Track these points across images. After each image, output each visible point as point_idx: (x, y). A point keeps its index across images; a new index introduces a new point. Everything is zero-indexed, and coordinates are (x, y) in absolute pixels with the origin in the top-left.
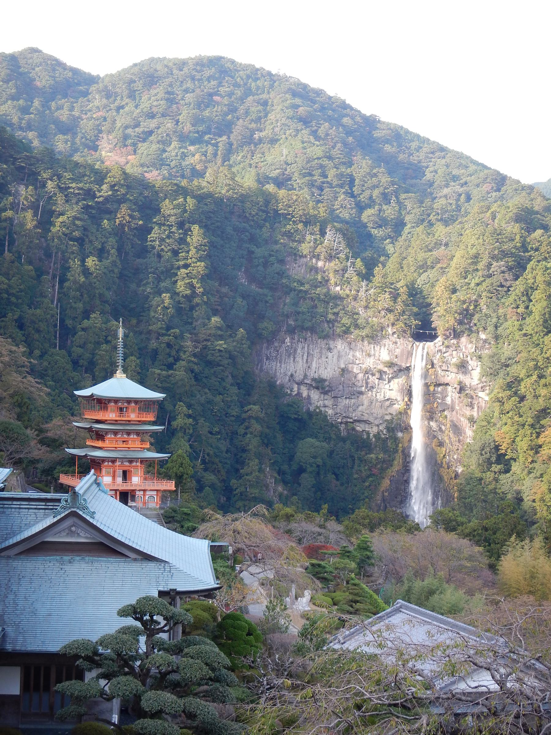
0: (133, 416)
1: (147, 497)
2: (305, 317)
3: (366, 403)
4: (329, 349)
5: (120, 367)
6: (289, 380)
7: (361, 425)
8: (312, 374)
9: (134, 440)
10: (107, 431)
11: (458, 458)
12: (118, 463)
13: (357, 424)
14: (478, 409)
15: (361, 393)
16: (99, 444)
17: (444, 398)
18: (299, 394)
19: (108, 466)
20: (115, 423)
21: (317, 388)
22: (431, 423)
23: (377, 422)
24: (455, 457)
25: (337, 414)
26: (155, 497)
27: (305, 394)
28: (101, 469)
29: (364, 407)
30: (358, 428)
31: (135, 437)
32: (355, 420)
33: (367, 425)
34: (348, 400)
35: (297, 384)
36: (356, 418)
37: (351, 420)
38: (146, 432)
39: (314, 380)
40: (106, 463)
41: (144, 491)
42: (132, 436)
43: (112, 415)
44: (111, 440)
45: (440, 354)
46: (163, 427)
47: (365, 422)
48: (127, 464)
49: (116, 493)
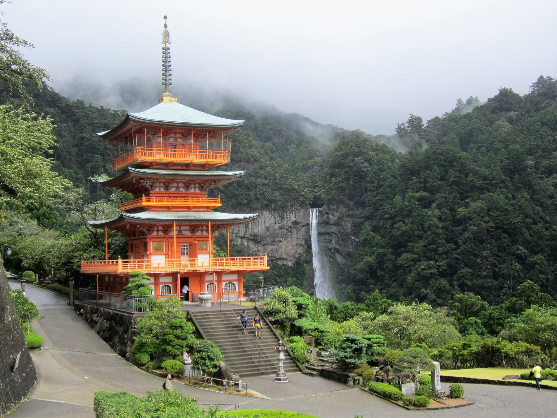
1: (224, 284)
2: (243, 197)
3: (283, 247)
6: (236, 237)
8: (250, 232)
9: (195, 196)
10: (155, 179)
12: (175, 233)
15: (280, 241)
18: (242, 244)
19: (157, 238)
20: (167, 165)
21: (253, 240)
23: (290, 259)
26: (236, 283)
27: (246, 244)
28: (145, 244)
29: (283, 249)
30: (279, 263)
31: (197, 191)
35: (241, 238)
38: (215, 180)
39: (250, 235)
40: (155, 233)
41: (219, 274)
42: (192, 190)
44: (160, 196)
46: (245, 171)
47: (284, 259)
49: (175, 280)
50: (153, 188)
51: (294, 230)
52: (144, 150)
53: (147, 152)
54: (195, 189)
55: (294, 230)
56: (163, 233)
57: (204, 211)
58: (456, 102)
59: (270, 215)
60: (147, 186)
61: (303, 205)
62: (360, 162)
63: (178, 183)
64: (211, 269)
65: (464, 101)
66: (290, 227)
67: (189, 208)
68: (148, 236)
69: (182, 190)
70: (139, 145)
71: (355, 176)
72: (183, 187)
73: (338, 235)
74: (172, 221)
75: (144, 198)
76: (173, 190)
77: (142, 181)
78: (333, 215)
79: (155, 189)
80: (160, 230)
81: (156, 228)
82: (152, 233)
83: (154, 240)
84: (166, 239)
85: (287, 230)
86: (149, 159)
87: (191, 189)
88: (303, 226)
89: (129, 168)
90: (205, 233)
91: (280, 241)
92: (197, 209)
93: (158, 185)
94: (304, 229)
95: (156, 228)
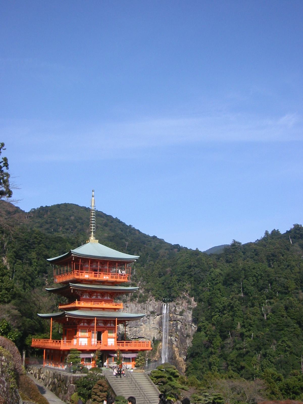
0: (106, 278)
3: (143, 329)
4: (127, 307)
5: (92, 233)
7: (142, 339)
9: (107, 301)
10: (84, 291)
11: (184, 352)
13: (140, 339)
14: (192, 331)
15: (141, 325)
16: (77, 304)
17: (177, 327)
22: (171, 338)
23: (148, 338)
24: (183, 352)
25: (131, 335)
31: (109, 298)
32: (139, 338)
33: (144, 339)
34: (136, 328)
36: (139, 336)
37: (137, 337)
40: (82, 324)
42: (106, 298)
43: (87, 276)
44: (86, 300)
45: (174, 308)
47: (143, 338)
48: (101, 325)
50: (82, 296)
51: (151, 318)
52: (78, 272)
53: (81, 273)
54: (107, 297)
55: (151, 318)
56: (87, 324)
57: (112, 311)
58: (265, 232)
59: (135, 306)
60: (79, 294)
61: (157, 299)
62: (198, 272)
63: (97, 293)
64: (116, 348)
65: (270, 232)
66: (149, 315)
67: (103, 309)
68: (78, 326)
69: (99, 297)
70: (75, 270)
71: (195, 281)
72: (100, 296)
73: (182, 322)
74: (94, 317)
75: (77, 302)
76: (94, 297)
77: (76, 291)
78: (179, 308)
79: (83, 296)
80: (85, 322)
81: (83, 321)
82: (81, 324)
83: (82, 328)
84: (88, 328)
85: (147, 317)
86: (81, 277)
87: (105, 297)
88: (158, 315)
89: (70, 283)
90: (112, 325)
91: (141, 325)
92: (108, 310)
93: (85, 294)
94: (158, 317)
95: (83, 321)
